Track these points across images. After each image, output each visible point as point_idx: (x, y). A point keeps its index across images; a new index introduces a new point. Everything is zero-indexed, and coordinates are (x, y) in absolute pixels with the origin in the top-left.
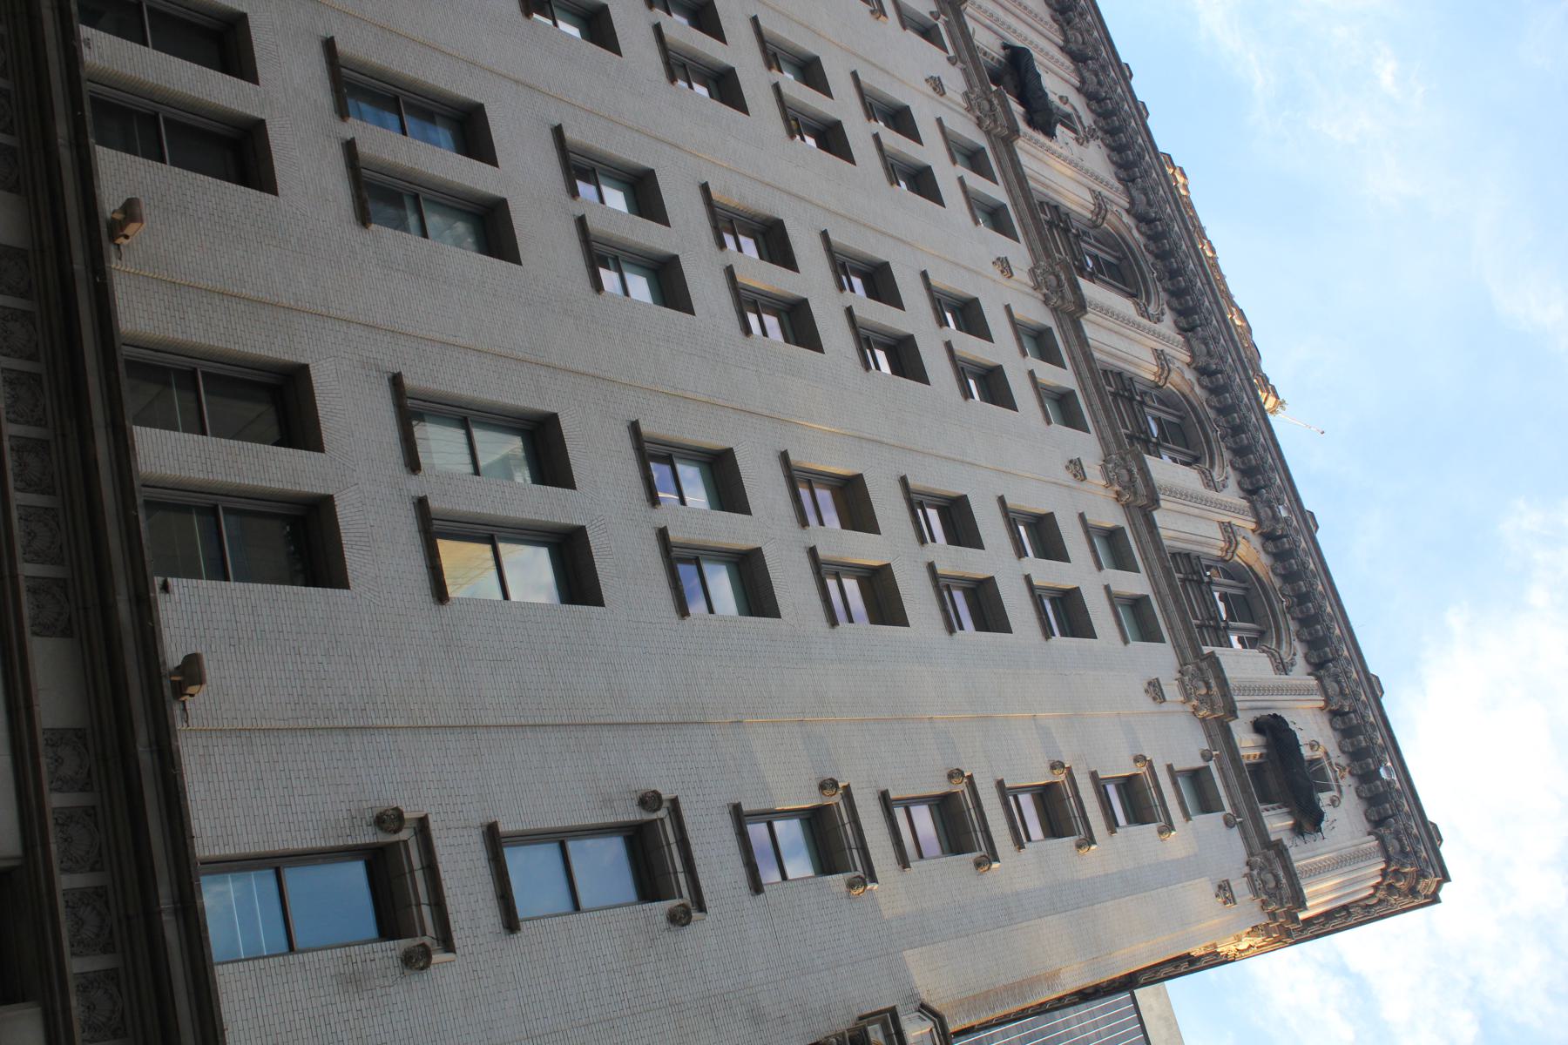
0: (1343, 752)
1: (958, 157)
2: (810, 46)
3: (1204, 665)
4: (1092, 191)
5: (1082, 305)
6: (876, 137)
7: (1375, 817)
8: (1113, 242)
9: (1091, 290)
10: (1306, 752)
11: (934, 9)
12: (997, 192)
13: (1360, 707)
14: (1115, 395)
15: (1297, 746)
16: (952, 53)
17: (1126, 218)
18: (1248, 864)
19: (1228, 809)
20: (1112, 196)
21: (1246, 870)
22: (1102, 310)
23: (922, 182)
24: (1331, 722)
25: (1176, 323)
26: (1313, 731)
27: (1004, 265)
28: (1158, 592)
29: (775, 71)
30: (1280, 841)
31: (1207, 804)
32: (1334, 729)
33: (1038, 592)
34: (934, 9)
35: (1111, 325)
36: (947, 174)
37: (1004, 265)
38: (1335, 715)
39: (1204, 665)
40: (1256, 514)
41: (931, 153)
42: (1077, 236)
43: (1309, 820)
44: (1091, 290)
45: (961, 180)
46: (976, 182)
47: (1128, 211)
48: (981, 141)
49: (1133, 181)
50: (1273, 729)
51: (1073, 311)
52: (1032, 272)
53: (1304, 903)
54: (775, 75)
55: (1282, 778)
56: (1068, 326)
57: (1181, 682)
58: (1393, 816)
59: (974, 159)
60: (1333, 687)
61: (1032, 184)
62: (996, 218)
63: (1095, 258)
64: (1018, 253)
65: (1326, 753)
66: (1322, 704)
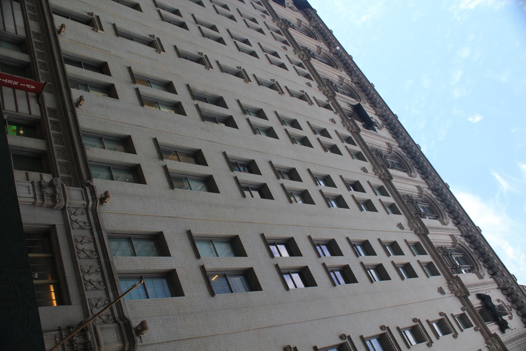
0: (509, 301)
3: (455, 280)
5: (391, 177)
8: (397, 156)
9: (392, 171)
10: (496, 303)
11: (327, 99)
12: (358, 148)
14: (407, 202)
19: (475, 326)
20: (392, 143)
21: (486, 345)
23: (334, 149)
24: (502, 292)
26: (497, 297)
27: (364, 170)
31: (467, 325)
32: (504, 294)
34: (327, 99)
36: (341, 146)
37: (364, 170)
38: (503, 289)
39: (455, 280)
40: (460, 230)
42: (385, 157)
43: (503, 326)
44: (392, 171)
49: (398, 137)
50: (484, 298)
51: (388, 179)
55: (489, 312)
59: (349, 140)
62: (359, 156)
64: (368, 165)
65: (503, 302)
66: (497, 287)
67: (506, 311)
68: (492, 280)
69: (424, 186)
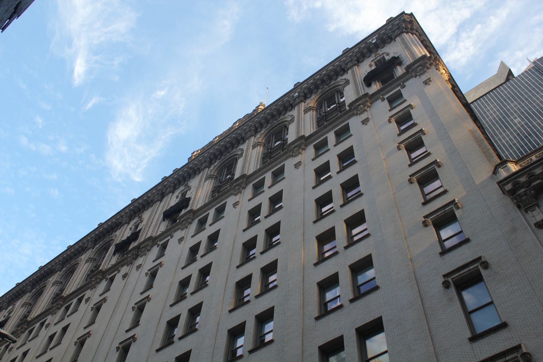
1: (203, 228)
2: (176, 286)
3: (353, 108)
4: (205, 181)
5: (243, 176)
6: (202, 257)
7: (389, 40)
8: (220, 171)
9: (237, 175)
10: (374, 67)
11: (156, 246)
12: (212, 212)
13: (354, 54)
14: (270, 158)
15: (372, 71)
16: (169, 237)
17: (212, 168)
18: (416, 77)
19: (399, 88)
21: (418, 77)
22: (243, 169)
23: (213, 238)
25: (242, 144)
26: (366, 67)
27: (235, 205)
28: (332, 129)
29: (187, 295)
30: (405, 68)
31: (399, 95)
32: (363, 61)
33: (342, 168)
34: (156, 246)
35: (248, 165)
36: (209, 230)
37: (235, 205)
39: (353, 108)
40: (299, 103)
41: (203, 237)
42: (221, 183)
43: (396, 61)
44: (237, 175)
45: (210, 225)
46: (210, 220)
47: (209, 168)
48: (196, 221)
49: (199, 169)
50: (369, 80)
51: (246, 179)
52: (236, 195)
53: (423, 56)
54: (188, 295)
56: (251, 179)
57: (360, 114)
58: (387, 35)
59: (202, 223)
60: (350, 64)
61: (207, 201)
62: (220, 211)
63: (227, 175)
64: (230, 201)
65: (372, 61)
66: (356, 66)
67: (380, 59)
68: (349, 72)
69: (253, 140)
